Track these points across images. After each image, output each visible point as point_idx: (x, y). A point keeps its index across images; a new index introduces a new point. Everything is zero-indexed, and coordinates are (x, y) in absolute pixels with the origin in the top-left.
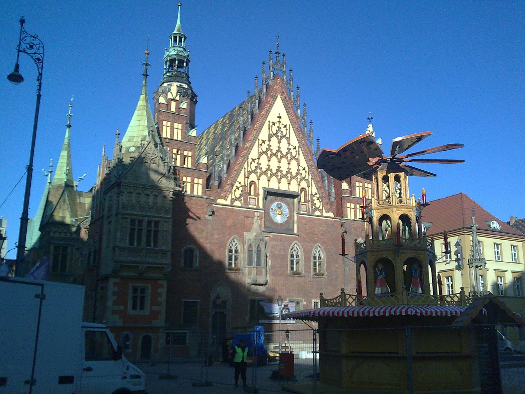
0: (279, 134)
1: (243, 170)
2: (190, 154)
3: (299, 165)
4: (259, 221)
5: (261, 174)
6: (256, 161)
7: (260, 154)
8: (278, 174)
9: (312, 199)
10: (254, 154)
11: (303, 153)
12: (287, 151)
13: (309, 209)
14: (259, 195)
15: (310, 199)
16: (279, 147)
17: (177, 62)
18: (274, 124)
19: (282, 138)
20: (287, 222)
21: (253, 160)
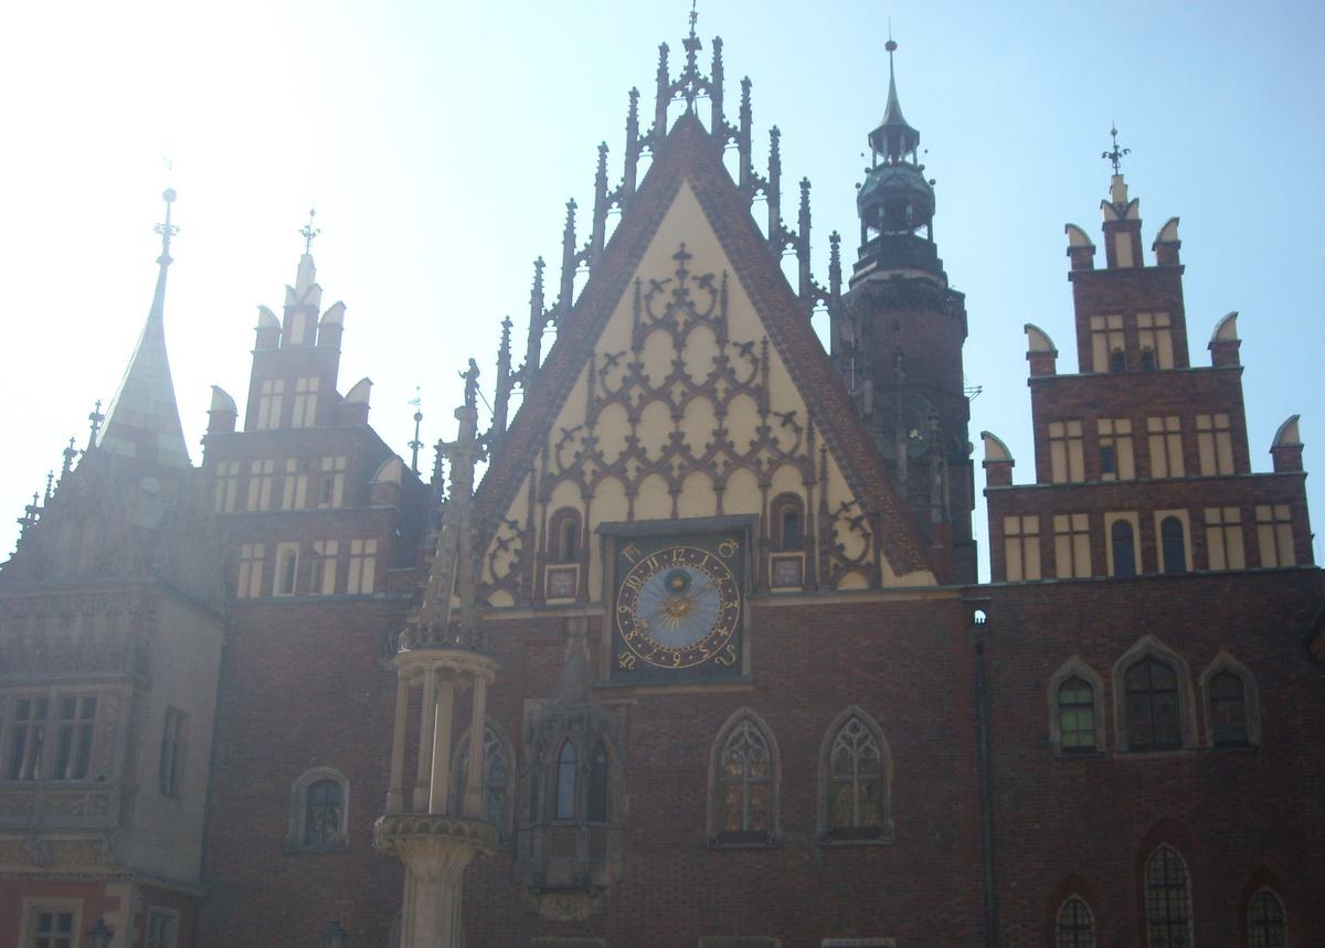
0: (681, 317)
1: (527, 480)
2: (341, 463)
3: (764, 411)
4: (587, 653)
5: (598, 477)
6: (578, 436)
7: (594, 409)
8: (675, 464)
9: (822, 532)
10: (572, 413)
11: (786, 361)
12: (712, 368)
13: (811, 573)
14: (587, 553)
15: (816, 534)
16: (678, 365)
17: (910, 210)
18: (657, 286)
19: (689, 326)
20: (713, 641)
21: (568, 435)
